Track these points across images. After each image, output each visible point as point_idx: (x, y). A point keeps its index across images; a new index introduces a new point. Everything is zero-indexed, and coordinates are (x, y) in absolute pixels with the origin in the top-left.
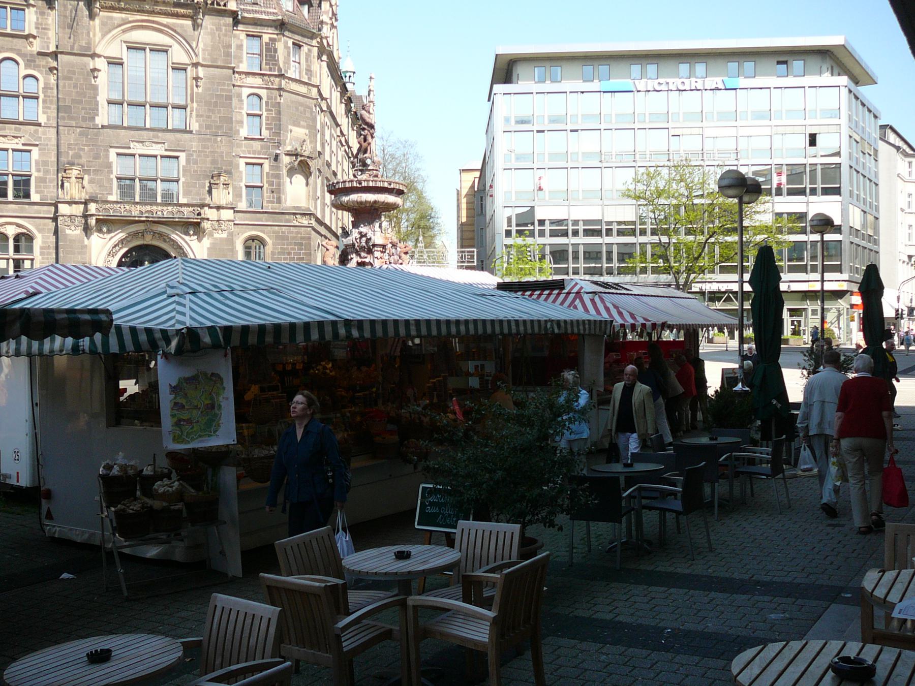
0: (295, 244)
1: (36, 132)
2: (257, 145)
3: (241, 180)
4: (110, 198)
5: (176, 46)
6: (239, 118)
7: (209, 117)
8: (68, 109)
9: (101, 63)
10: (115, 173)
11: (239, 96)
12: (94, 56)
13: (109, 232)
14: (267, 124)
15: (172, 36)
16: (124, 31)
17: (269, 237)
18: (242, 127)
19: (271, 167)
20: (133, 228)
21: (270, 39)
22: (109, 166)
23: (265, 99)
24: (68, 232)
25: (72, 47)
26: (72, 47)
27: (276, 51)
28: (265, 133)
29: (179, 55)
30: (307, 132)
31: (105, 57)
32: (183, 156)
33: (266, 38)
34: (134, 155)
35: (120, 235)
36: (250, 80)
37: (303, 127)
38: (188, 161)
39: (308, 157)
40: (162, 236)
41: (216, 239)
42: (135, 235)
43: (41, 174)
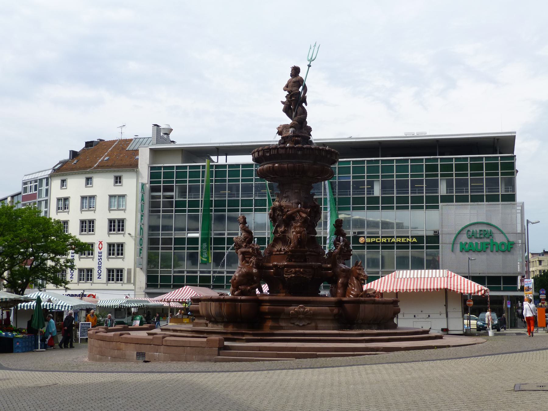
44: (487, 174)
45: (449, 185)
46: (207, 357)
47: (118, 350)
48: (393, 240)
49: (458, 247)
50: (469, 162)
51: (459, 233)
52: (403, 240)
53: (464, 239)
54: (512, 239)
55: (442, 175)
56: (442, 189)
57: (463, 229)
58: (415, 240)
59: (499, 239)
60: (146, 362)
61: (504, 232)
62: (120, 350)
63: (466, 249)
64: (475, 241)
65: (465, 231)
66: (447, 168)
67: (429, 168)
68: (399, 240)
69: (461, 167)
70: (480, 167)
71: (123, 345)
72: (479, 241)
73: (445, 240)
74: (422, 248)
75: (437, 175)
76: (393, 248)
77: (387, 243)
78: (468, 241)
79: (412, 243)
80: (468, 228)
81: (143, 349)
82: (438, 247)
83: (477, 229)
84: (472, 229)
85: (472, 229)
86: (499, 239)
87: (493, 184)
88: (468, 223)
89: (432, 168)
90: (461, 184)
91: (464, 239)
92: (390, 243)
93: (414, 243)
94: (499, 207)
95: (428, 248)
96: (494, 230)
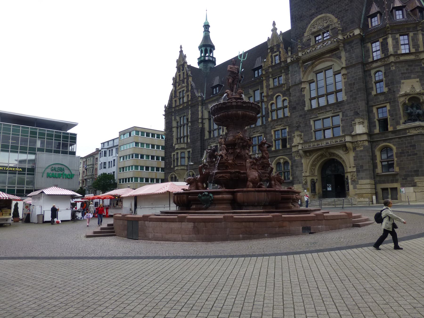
0: (411, 146)
1: (287, 120)
2: (382, 98)
3: (375, 118)
4: (312, 140)
5: (335, 64)
6: (370, 86)
7: (351, 91)
8: (295, 108)
9: (306, 86)
10: (313, 129)
11: (370, 74)
12: (301, 83)
13: (310, 155)
14: (386, 84)
15: (332, 61)
16: (313, 68)
17: (394, 145)
18: (373, 90)
19: (391, 106)
20: (319, 153)
21: (383, 39)
22: (311, 126)
23: (383, 71)
24: (296, 158)
25: (295, 83)
26: (295, 83)
27: (387, 44)
28: (385, 90)
29: (337, 68)
30: (418, 80)
31: (307, 82)
32: (341, 114)
33: (381, 40)
34: (320, 119)
35: (314, 156)
36: (374, 65)
37: (415, 78)
38: (343, 116)
39: (417, 94)
40: (334, 154)
41: (358, 151)
42: (322, 156)
43: (289, 137)
44: (63, 141)
45: (42, 143)
46: (349, 225)
47: (279, 227)
48: (7, 169)
49: (45, 175)
50: (54, 133)
51: (47, 168)
52: (13, 169)
53: (49, 171)
54: (73, 172)
55: (39, 138)
56: (38, 144)
57: (49, 166)
58: (21, 169)
59: (67, 172)
60: (310, 233)
61: (70, 169)
62: (283, 227)
63: (48, 176)
64: (54, 172)
65: (50, 167)
66: (42, 134)
67: (32, 133)
68: (11, 169)
69: (50, 136)
70: (60, 137)
71: (286, 224)
72: (57, 173)
73: (38, 171)
74: (25, 174)
75: (36, 137)
76: (6, 173)
77: (3, 170)
78: (52, 172)
79: (18, 171)
80: (52, 166)
81: (308, 224)
82: (33, 174)
83: (57, 166)
84: (54, 166)
85: (54, 166)
86: (67, 172)
87: (65, 146)
88: (52, 163)
89: (33, 133)
90: (49, 144)
91: (49, 171)
92: (5, 170)
93: (20, 171)
94: (68, 157)
95: (28, 174)
96: (65, 168)
